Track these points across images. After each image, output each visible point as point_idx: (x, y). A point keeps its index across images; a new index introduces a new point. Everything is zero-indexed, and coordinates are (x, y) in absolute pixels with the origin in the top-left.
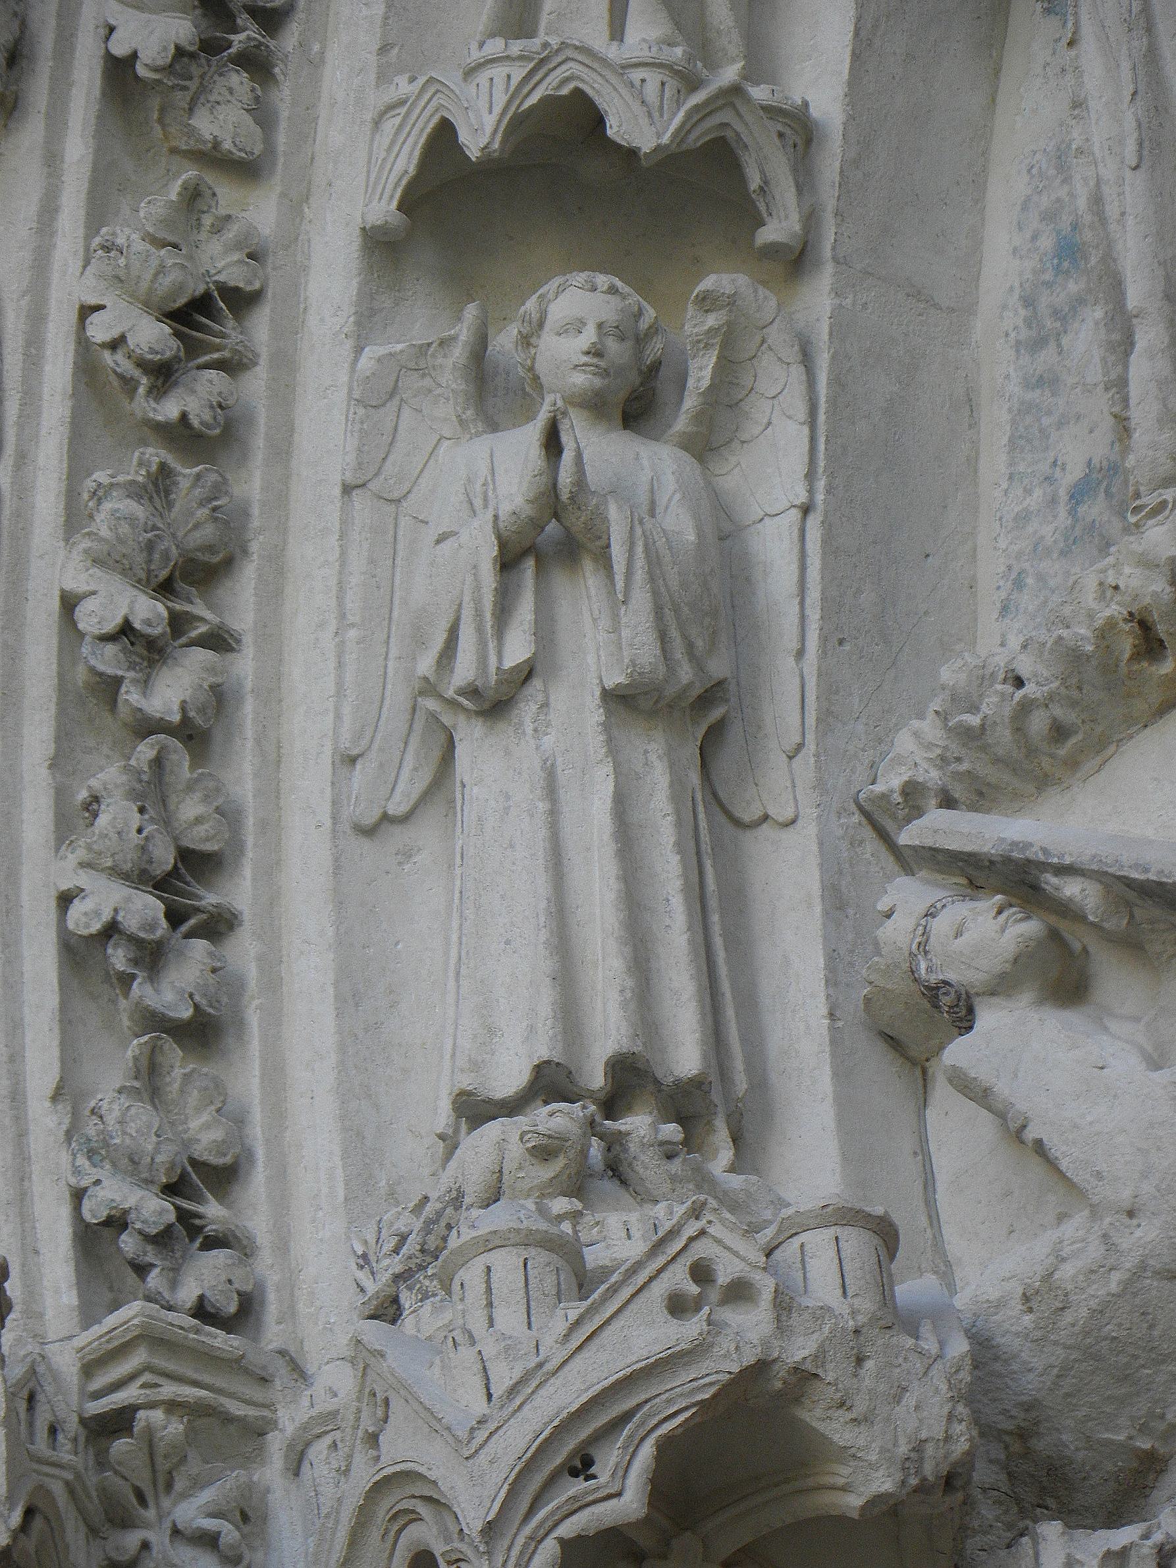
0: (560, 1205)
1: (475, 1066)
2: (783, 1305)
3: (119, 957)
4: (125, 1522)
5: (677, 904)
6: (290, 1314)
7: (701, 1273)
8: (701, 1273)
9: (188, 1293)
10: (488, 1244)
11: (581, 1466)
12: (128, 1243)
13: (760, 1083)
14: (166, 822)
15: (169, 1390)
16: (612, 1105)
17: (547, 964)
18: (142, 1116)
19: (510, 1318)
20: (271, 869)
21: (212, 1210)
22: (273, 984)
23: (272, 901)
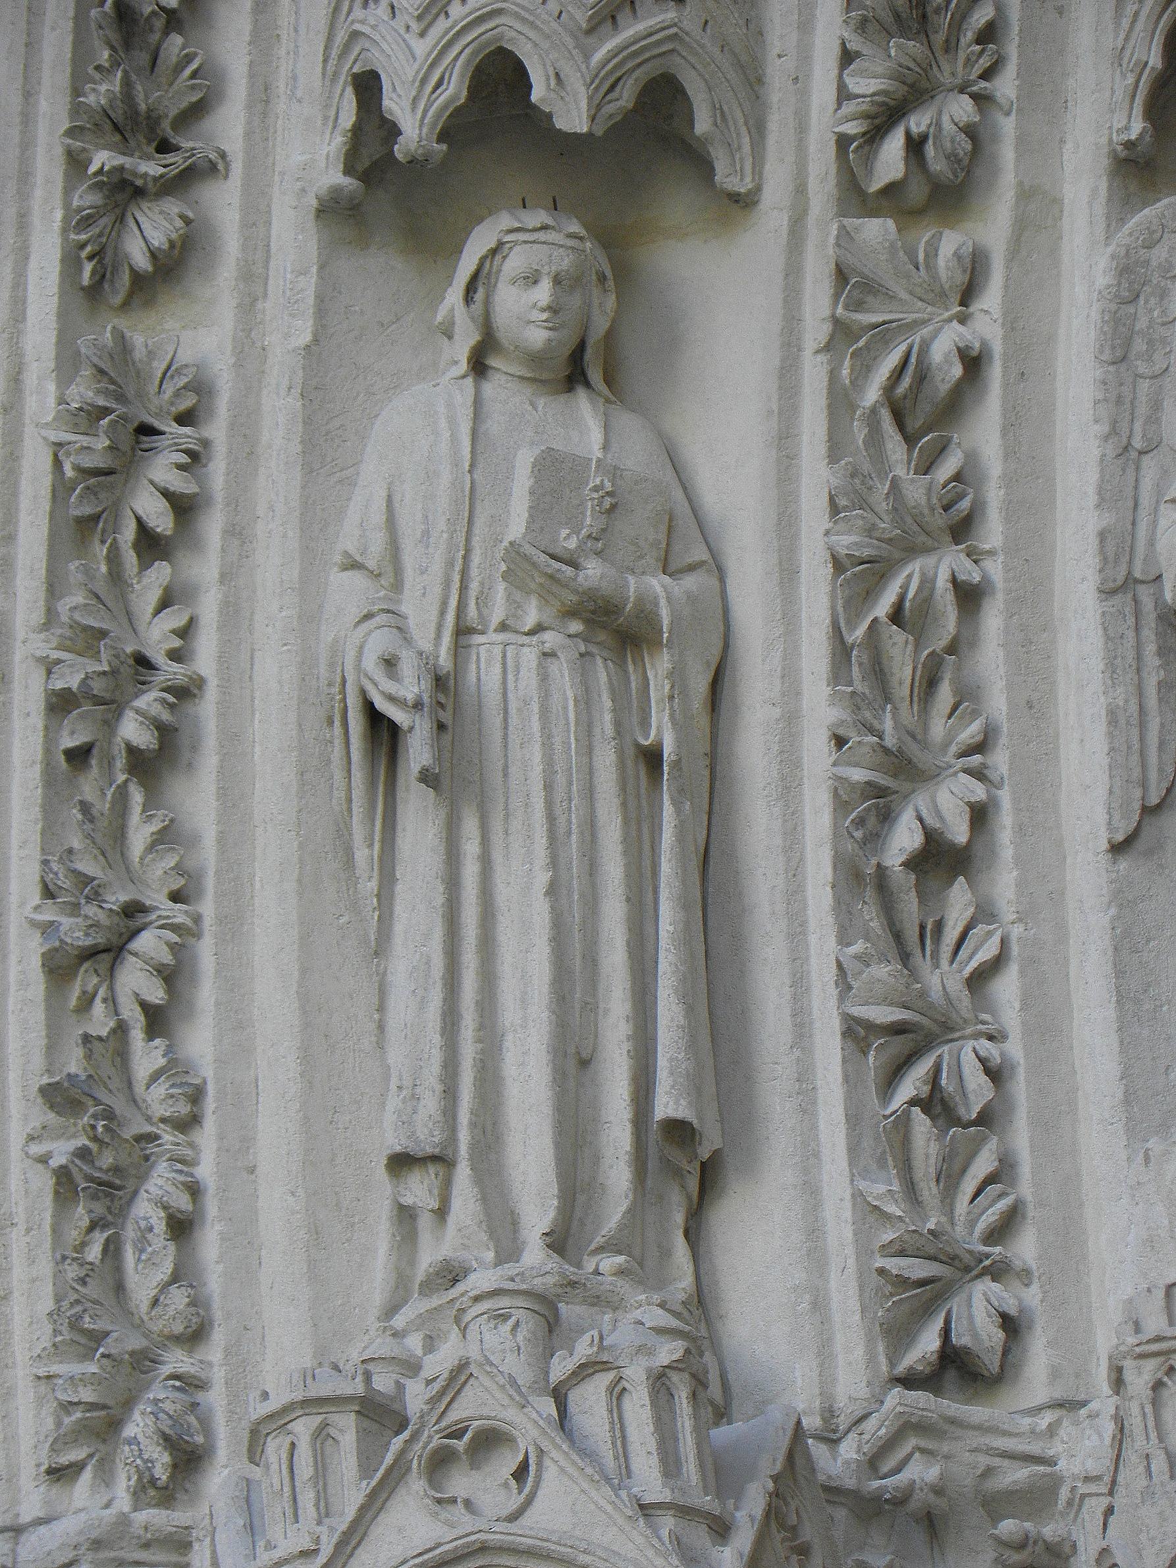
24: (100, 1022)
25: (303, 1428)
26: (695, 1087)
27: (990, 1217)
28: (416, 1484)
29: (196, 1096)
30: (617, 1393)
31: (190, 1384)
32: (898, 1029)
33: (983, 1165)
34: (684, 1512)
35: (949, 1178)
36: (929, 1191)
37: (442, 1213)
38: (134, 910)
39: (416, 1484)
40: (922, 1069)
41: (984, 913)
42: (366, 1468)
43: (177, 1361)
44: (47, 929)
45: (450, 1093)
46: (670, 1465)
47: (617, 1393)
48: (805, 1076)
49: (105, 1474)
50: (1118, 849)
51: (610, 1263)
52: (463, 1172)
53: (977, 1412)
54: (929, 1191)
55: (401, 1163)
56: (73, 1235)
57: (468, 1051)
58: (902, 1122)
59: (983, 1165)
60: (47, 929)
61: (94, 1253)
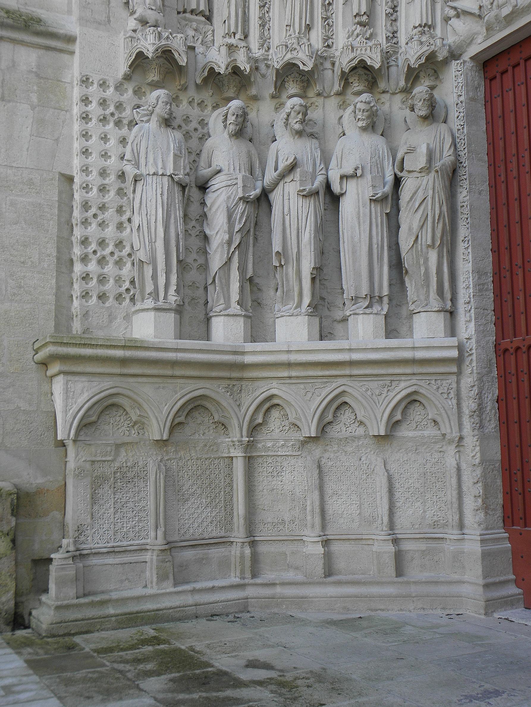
0: (420, 36)
1: (415, 24)
2: (435, 46)
3: (389, 15)
4: (389, 59)
5: (430, 10)
6: (401, 43)
7: (430, 43)
8: (430, 43)
9: (393, 42)
10: (414, 41)
11: (420, 58)
12: (389, 38)
13: (435, 24)
14: (393, 3)
15: (392, 50)
16: (424, 27)
17: (420, 16)
18: (391, 28)
19: (416, 47)
20: (401, 6)
21: (395, 35)
22: (400, 16)
23: (401, 9)
24: (263, 12)
25: (281, 47)
26: (310, 21)
27: (332, 34)
28: (290, 52)
29: (270, 19)
30: (305, 46)
31: (269, 43)
32: (325, 18)
33: (331, 30)
34: (310, 56)
35: (329, 31)
36: (327, 31)
37: (290, 30)
38: (266, 3)
39: (290, 52)
40: (327, 21)
41: (333, 9)
42: (286, 51)
43: (268, 40)
44: (259, 4)
45: (291, 20)
46: (309, 52)
47: (305, 46)
48: (318, 21)
49: (263, 49)
50: (343, 4)
51: (302, 35)
52: (292, 27)
53: (330, 50)
54: (327, 31)
55: (287, 26)
56: (260, 30)
57: (293, 17)
58: (326, 25)
59: (331, 30)
60: (259, 4)
61: (262, 31)
